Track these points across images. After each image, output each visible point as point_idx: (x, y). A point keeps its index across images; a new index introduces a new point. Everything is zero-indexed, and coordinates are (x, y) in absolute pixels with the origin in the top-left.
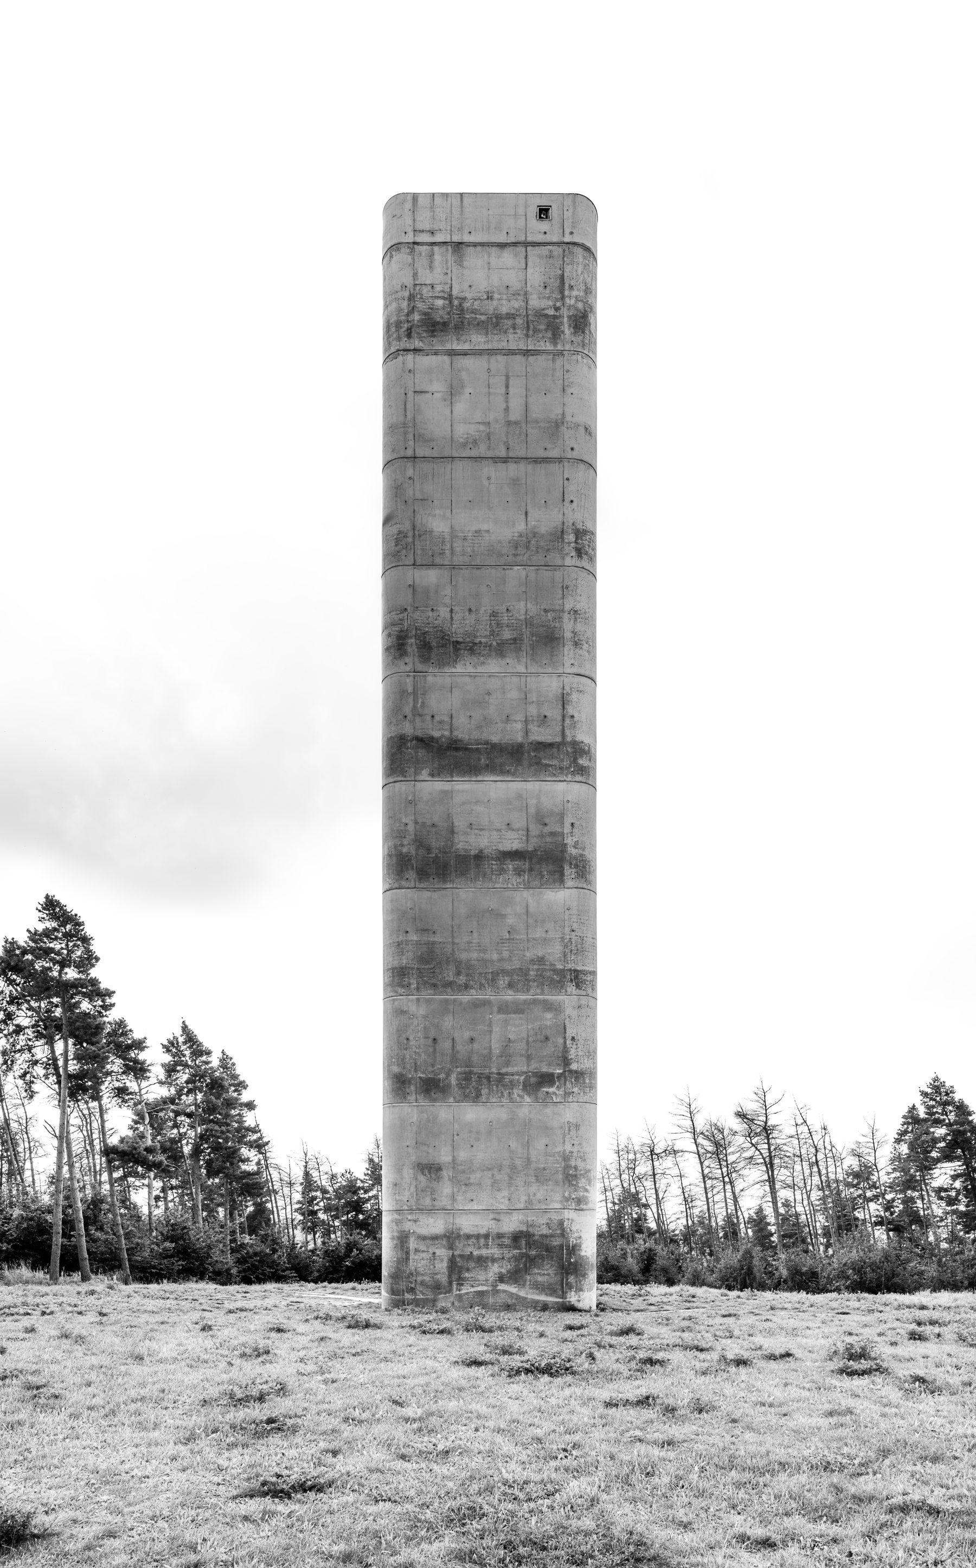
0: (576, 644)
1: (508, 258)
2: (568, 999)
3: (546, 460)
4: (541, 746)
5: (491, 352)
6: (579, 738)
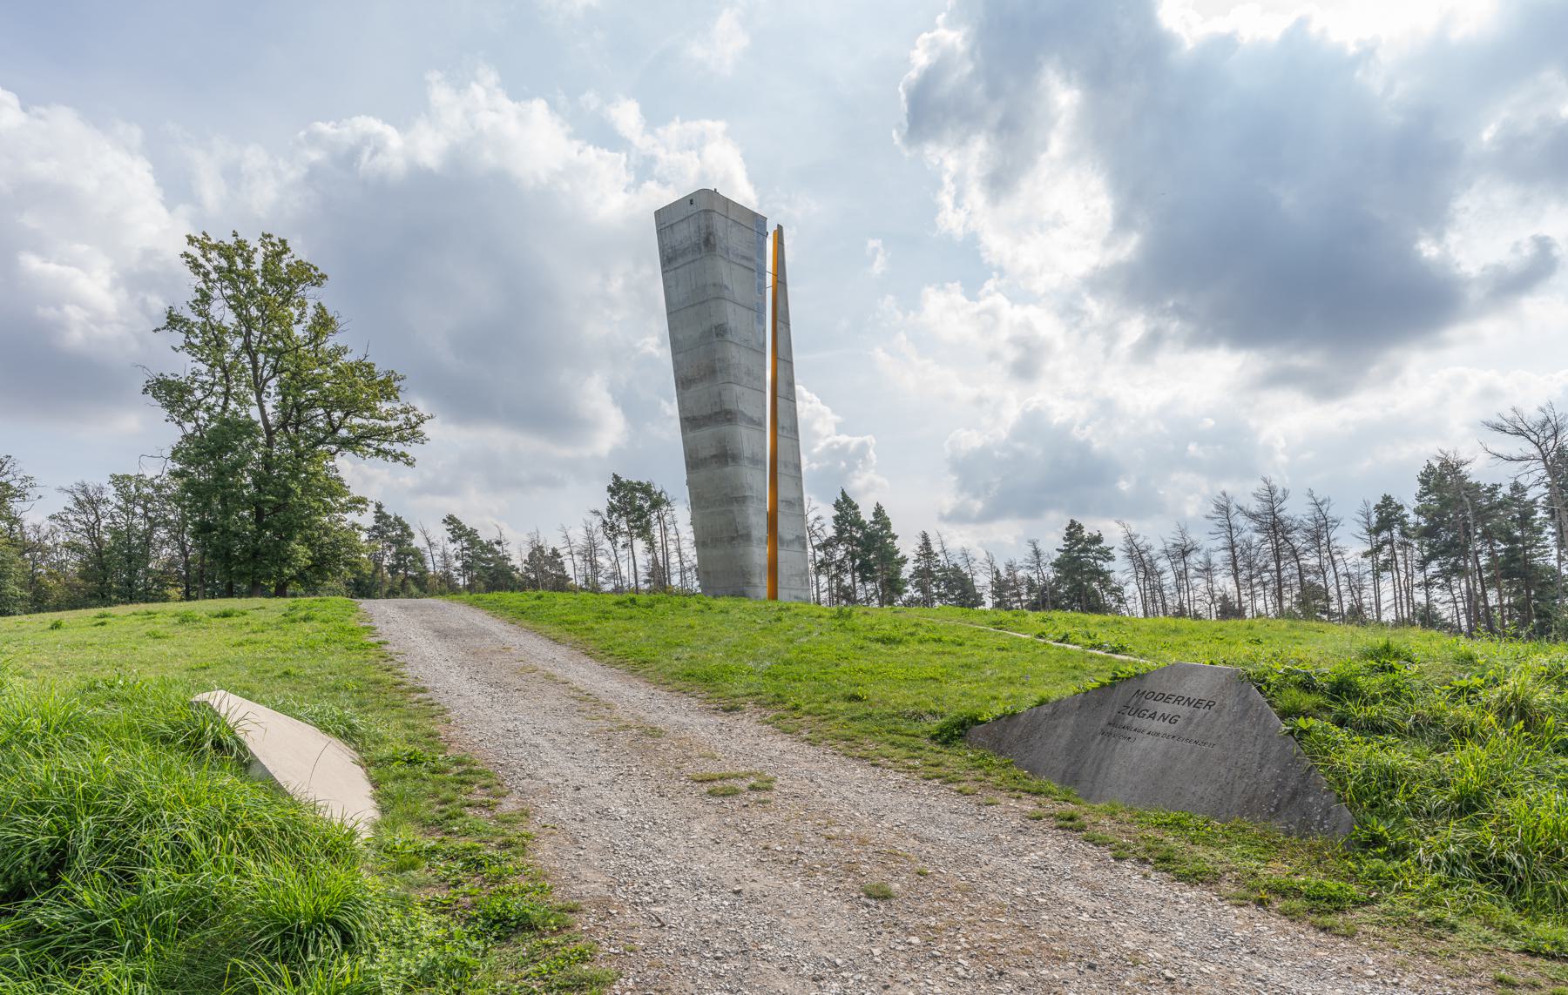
0: (721, 372)
1: (684, 225)
2: (735, 508)
3: (704, 302)
4: (716, 413)
5: (685, 264)
6: (727, 407)
